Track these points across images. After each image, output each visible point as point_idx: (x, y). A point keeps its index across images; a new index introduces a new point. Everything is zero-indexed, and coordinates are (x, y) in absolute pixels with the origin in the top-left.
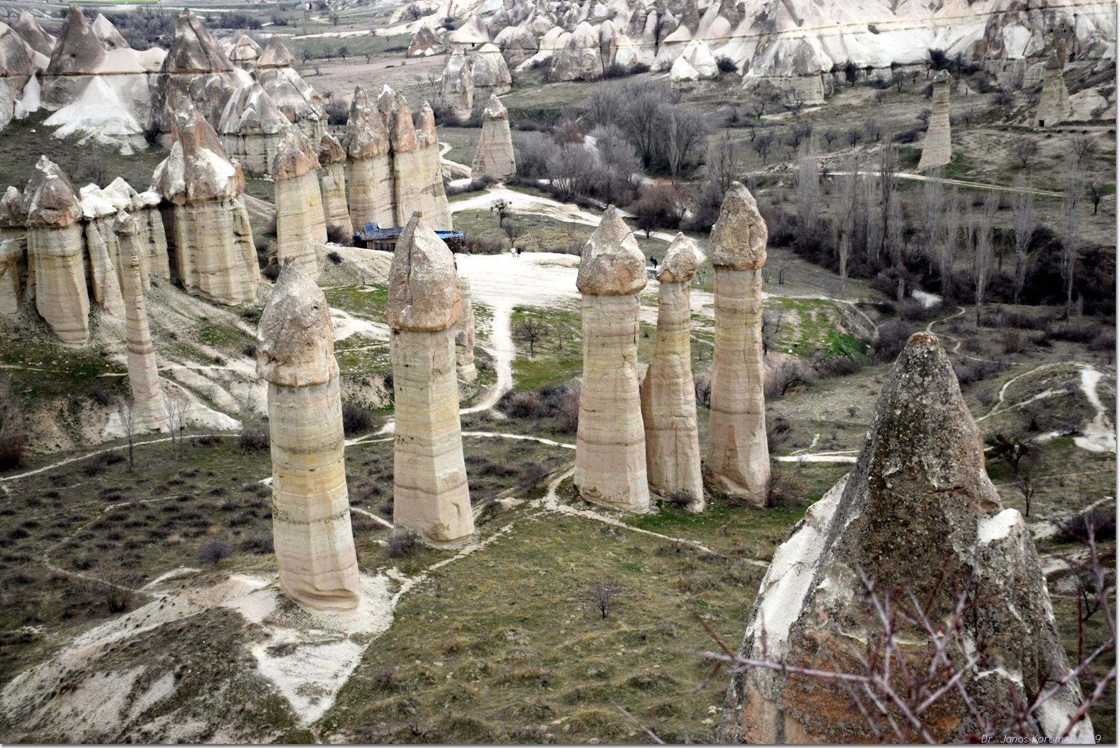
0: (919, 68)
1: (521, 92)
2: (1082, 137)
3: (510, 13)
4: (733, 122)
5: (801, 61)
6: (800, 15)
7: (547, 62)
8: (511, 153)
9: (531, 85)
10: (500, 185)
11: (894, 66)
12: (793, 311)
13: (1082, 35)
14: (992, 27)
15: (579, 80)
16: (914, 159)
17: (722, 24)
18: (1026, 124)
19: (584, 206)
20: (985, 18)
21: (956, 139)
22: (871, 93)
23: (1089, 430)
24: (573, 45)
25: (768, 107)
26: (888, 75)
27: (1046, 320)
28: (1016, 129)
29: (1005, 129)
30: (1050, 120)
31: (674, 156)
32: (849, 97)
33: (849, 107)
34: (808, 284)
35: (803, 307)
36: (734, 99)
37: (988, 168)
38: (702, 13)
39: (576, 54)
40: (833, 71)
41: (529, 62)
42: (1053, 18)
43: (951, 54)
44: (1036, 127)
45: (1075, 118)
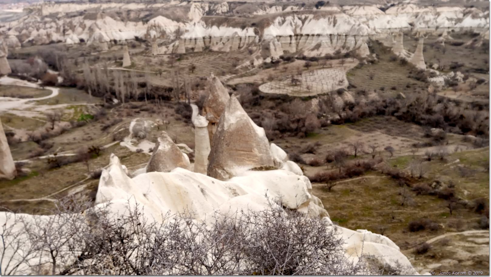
0: (133, 41)
1: (25, 49)
2: (160, 58)
3: (25, 26)
4: (82, 55)
5: (101, 39)
6: (100, 27)
7: (33, 40)
8: (9, 67)
9: (27, 46)
10: (6, 76)
11: (126, 40)
12: (73, 109)
13: (167, 32)
14: (148, 31)
15: (42, 44)
16: (121, 64)
17: (80, 29)
18: (150, 55)
19: (29, 81)
20: (147, 28)
21: (131, 59)
22: (119, 47)
23: (126, 139)
24: (39, 35)
25: (93, 51)
26: (124, 42)
27: (141, 106)
28: (148, 56)
29: (145, 56)
30: (155, 54)
31: (58, 66)
32: (115, 48)
33: (114, 51)
34: (84, 100)
35: (76, 108)
36: (84, 49)
37: (140, 66)
38: (75, 26)
39: (40, 38)
40: (111, 41)
41: (27, 40)
42: (160, 29)
43: (140, 37)
44: (152, 55)
45: (161, 53)
